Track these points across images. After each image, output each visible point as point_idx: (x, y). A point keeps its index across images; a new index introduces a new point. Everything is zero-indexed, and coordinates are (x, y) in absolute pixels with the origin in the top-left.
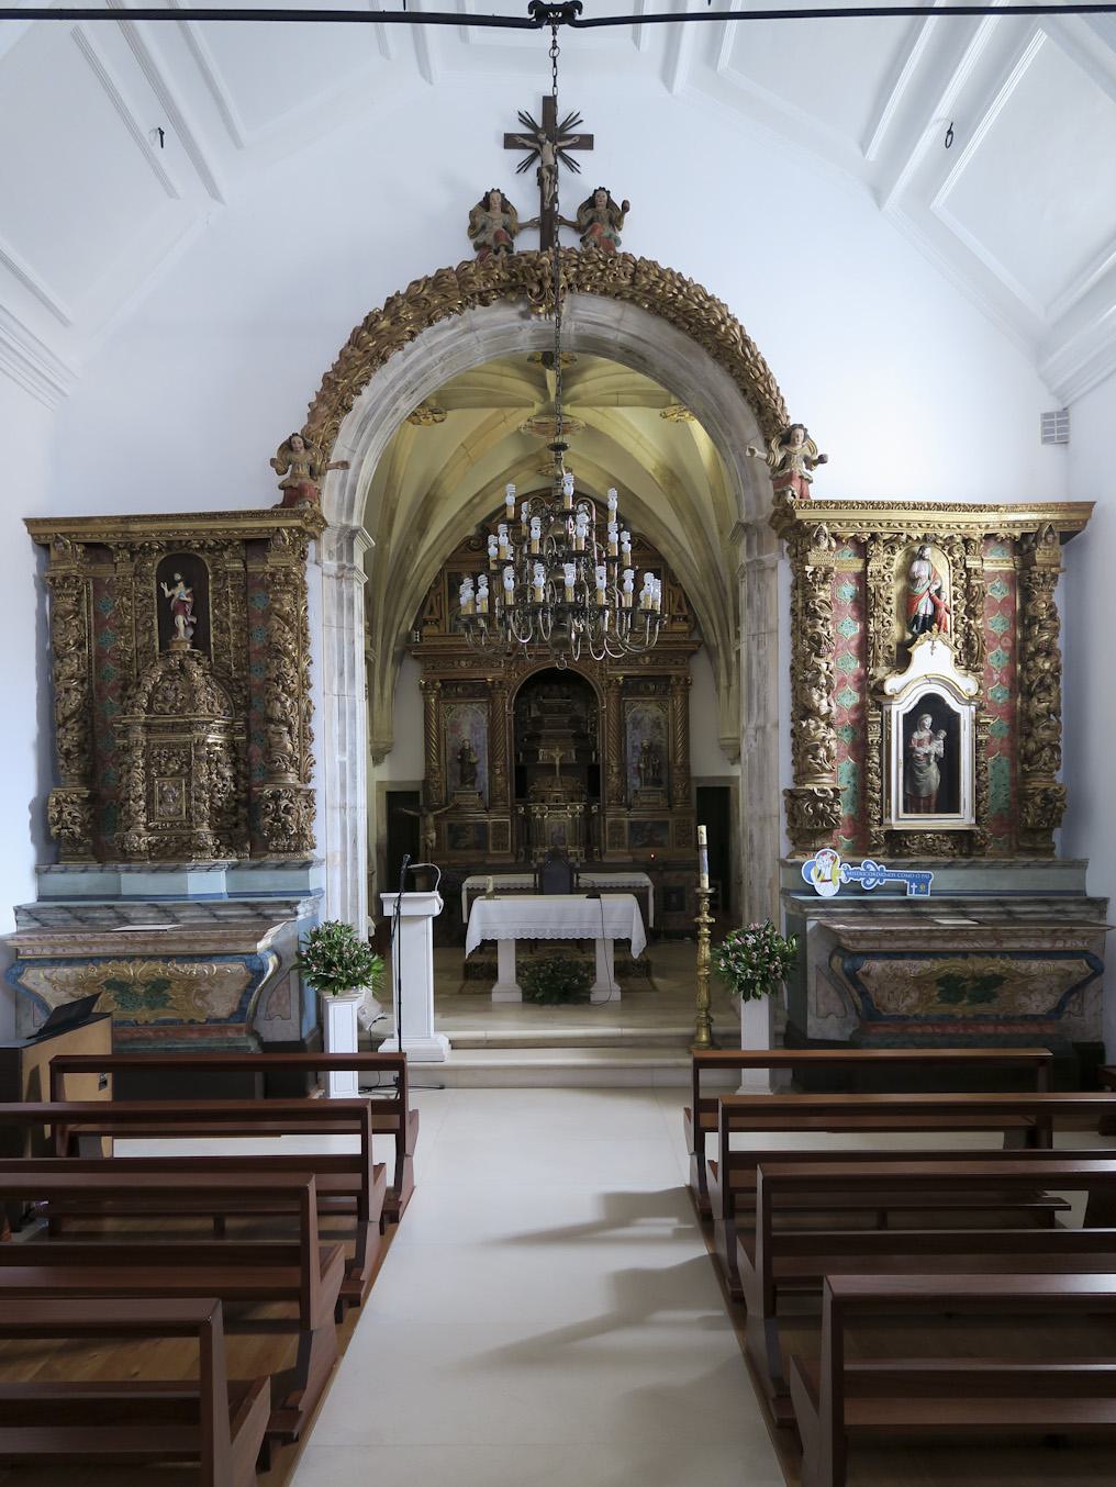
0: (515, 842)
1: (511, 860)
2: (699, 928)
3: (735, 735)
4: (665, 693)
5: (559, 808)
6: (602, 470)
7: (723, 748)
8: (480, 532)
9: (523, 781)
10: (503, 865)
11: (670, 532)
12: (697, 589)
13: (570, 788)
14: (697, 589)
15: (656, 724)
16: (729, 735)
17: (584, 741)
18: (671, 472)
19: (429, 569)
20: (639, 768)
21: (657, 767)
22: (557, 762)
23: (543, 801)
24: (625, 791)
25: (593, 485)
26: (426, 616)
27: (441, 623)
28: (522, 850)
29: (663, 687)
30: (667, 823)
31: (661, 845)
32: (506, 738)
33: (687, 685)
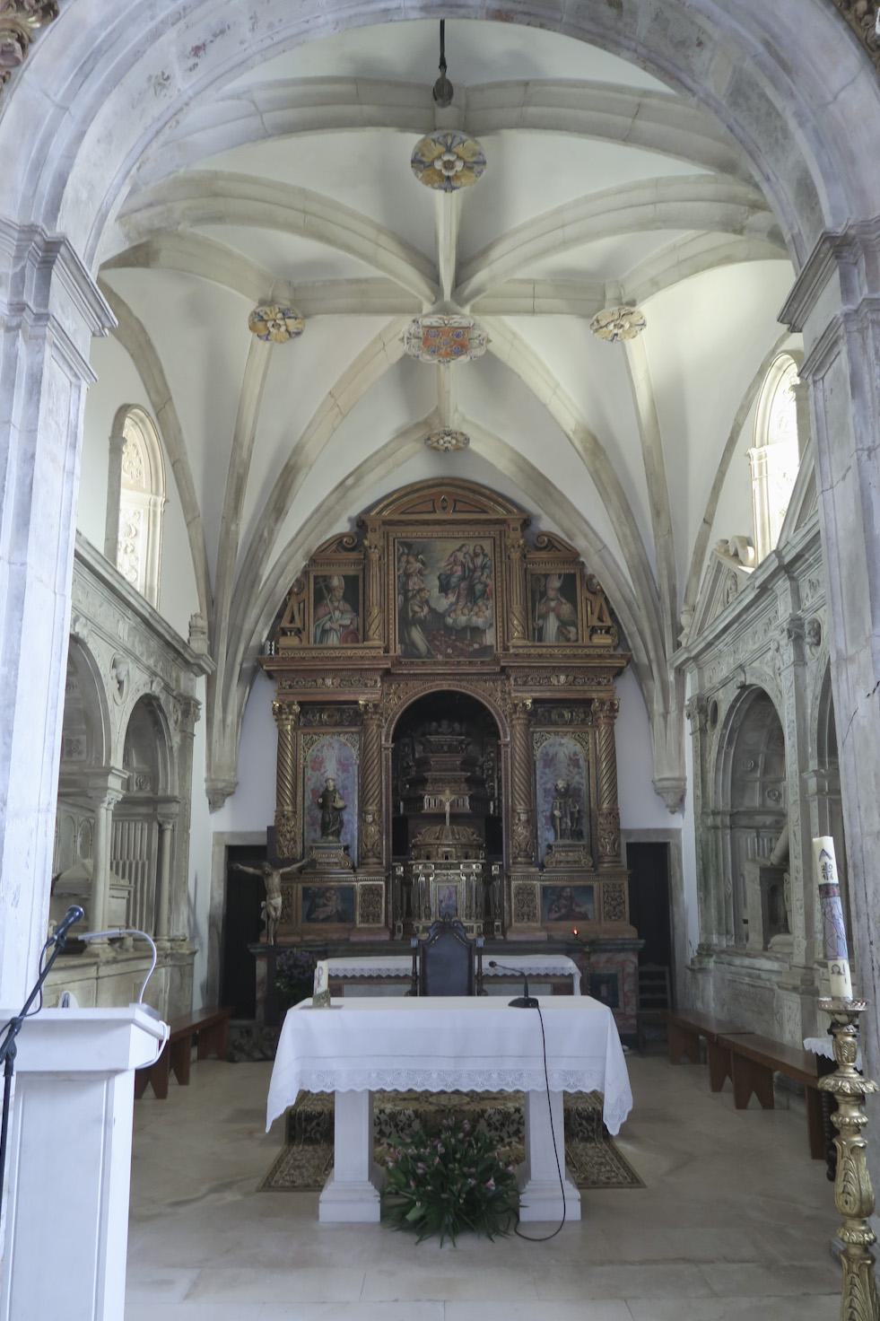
0: (390, 914)
1: (385, 937)
2: (834, 1107)
3: (677, 775)
4: (583, 722)
5: (451, 867)
6: (506, 445)
7: (659, 792)
8: (356, 529)
9: (402, 840)
10: (372, 943)
11: (586, 522)
12: (623, 596)
13: (463, 840)
14: (623, 596)
15: (574, 761)
16: (667, 775)
17: (481, 785)
18: (595, 439)
19: (290, 567)
20: (553, 816)
21: (576, 815)
22: (447, 808)
23: (428, 858)
24: (535, 846)
25: (495, 463)
26: (285, 624)
27: (304, 635)
28: (399, 924)
29: (582, 716)
30: (591, 888)
31: (584, 917)
32: (382, 778)
33: (613, 709)
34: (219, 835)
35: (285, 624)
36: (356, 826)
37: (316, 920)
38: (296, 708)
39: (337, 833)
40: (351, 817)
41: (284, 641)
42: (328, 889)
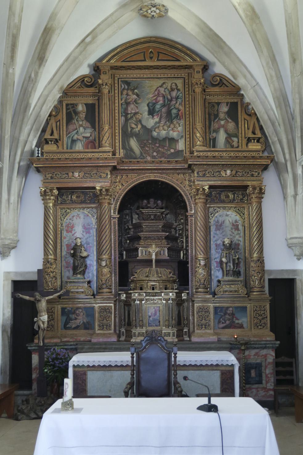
0: (117, 324)
1: (114, 339)
5: (156, 295)
7: (290, 246)
8: (93, 72)
10: (106, 343)
13: (164, 278)
15: (235, 226)
16: (295, 235)
20: (221, 262)
22: (154, 257)
23: (141, 289)
27: (60, 143)
28: (123, 330)
29: (241, 197)
30: (246, 307)
31: (241, 326)
33: (261, 192)
34: (7, 274)
35: (47, 136)
36: (95, 268)
37: (70, 328)
38: (56, 192)
39: (83, 273)
40: (92, 262)
41: (47, 148)
42: (78, 308)
